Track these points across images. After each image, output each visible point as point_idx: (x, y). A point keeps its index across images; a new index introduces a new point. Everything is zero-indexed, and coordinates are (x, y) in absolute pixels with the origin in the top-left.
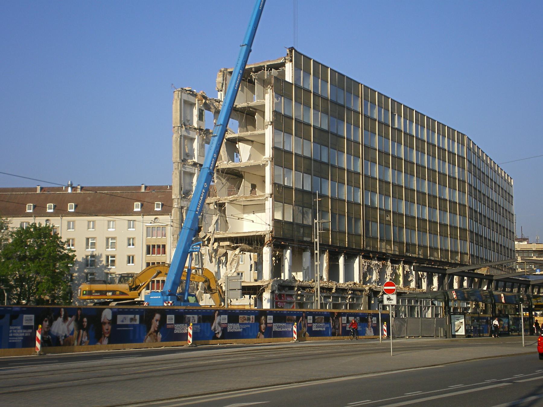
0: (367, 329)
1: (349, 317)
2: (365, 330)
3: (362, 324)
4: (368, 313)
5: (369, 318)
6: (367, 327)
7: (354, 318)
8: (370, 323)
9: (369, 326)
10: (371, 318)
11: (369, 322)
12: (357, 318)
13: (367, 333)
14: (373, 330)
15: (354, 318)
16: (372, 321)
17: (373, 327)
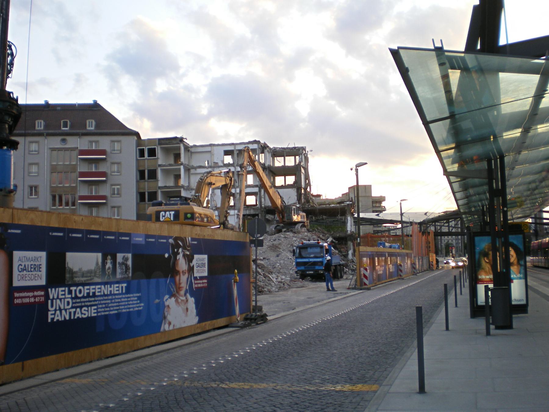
0: (171, 302)
1: (69, 255)
2: (161, 309)
3: (144, 282)
4: (176, 239)
5: (180, 257)
6: (172, 295)
7: (100, 255)
8: (183, 279)
9: (179, 289)
10: (189, 259)
11: (178, 273)
12: (120, 257)
13: (169, 318)
14: (197, 303)
15: (100, 255)
16: (191, 269)
17: (193, 292)
